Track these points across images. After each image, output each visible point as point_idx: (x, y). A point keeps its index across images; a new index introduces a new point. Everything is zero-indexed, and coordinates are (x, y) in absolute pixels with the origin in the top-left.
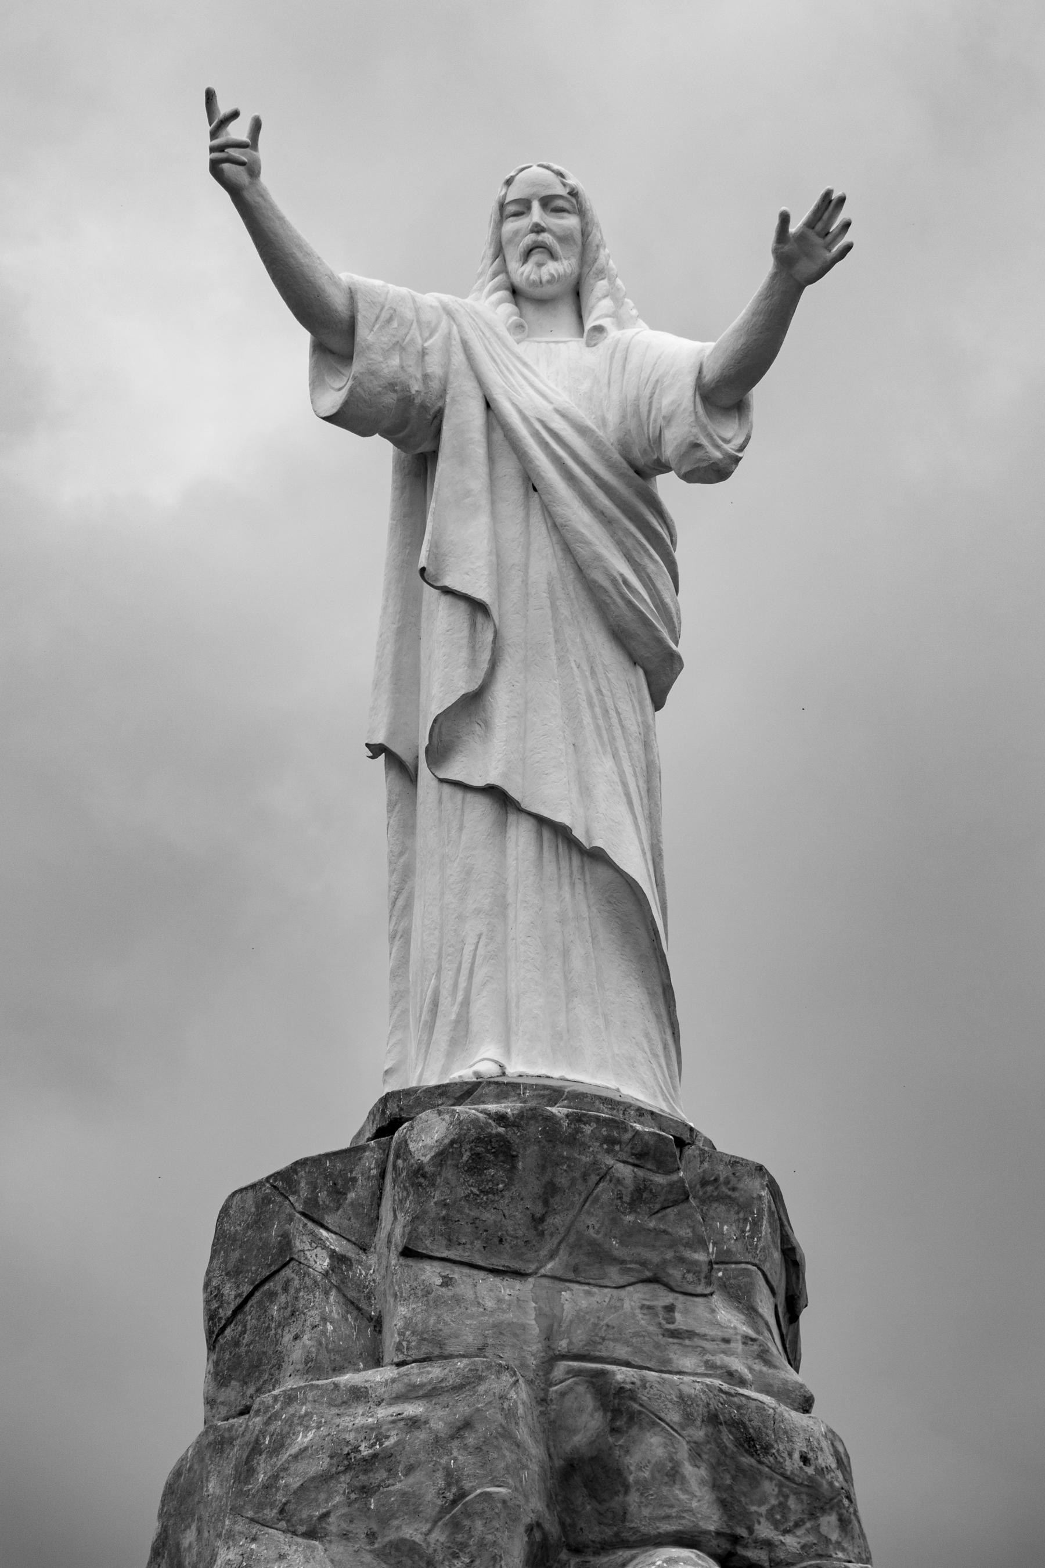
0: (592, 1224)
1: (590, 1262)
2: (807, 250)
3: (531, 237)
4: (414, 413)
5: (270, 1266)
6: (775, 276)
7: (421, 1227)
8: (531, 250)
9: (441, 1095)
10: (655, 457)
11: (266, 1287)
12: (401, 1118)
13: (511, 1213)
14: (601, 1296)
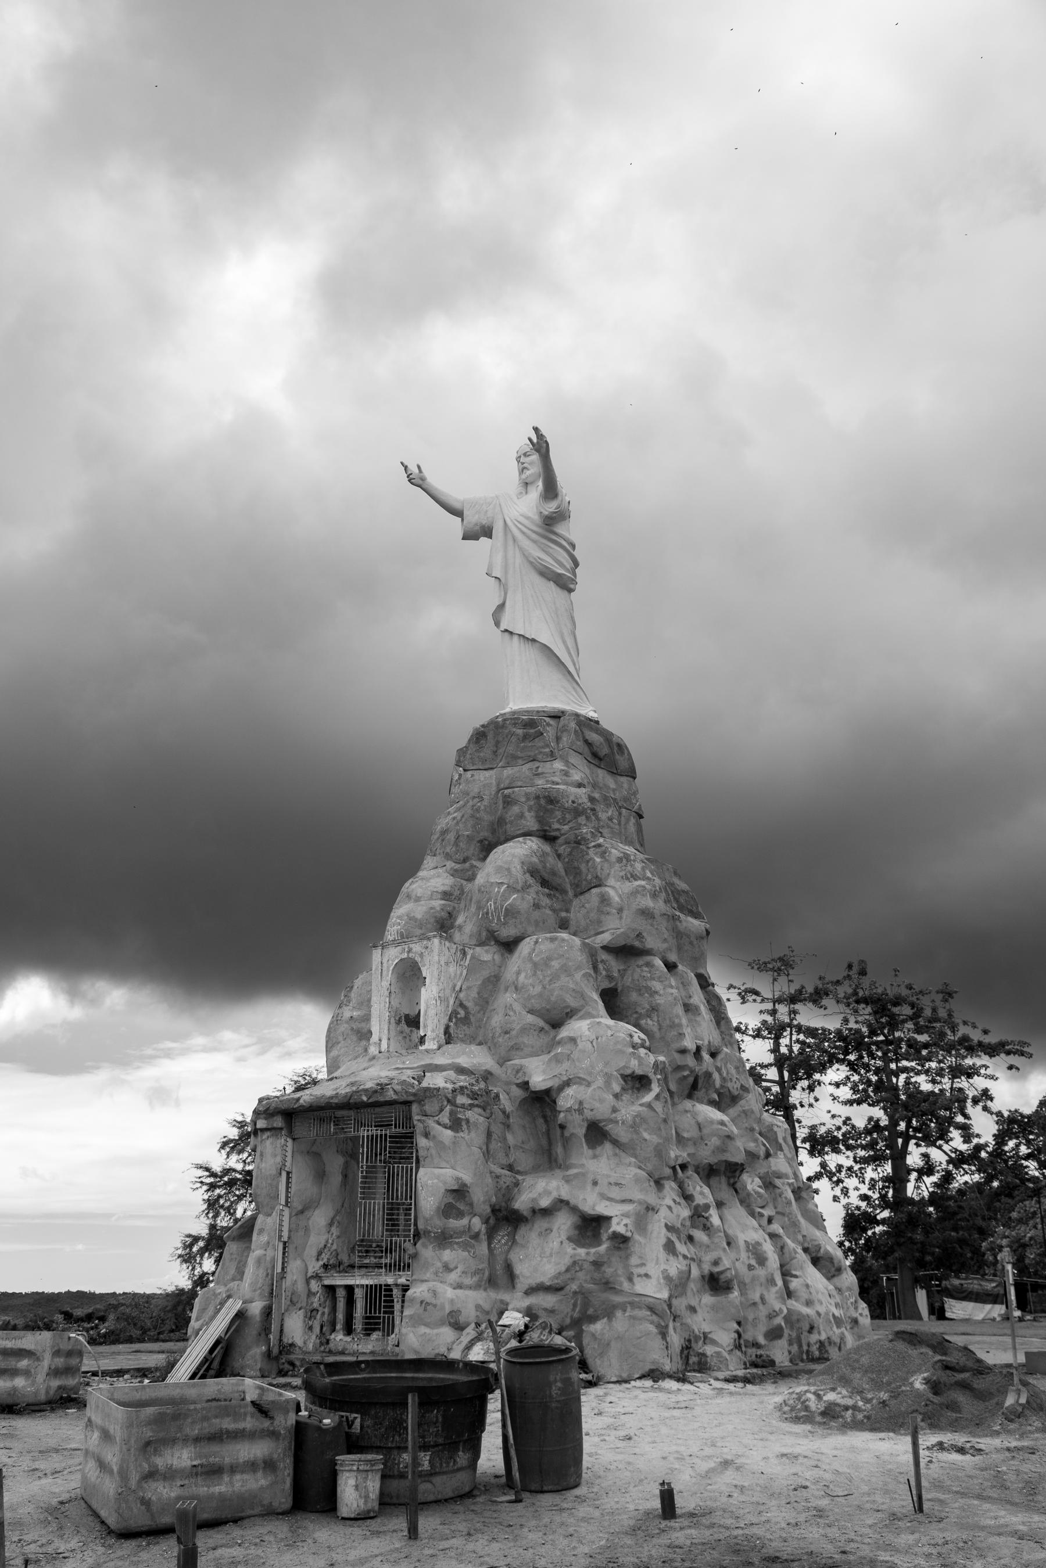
0: (511, 749)
1: (512, 760)
13: (486, 752)
14: (516, 769)
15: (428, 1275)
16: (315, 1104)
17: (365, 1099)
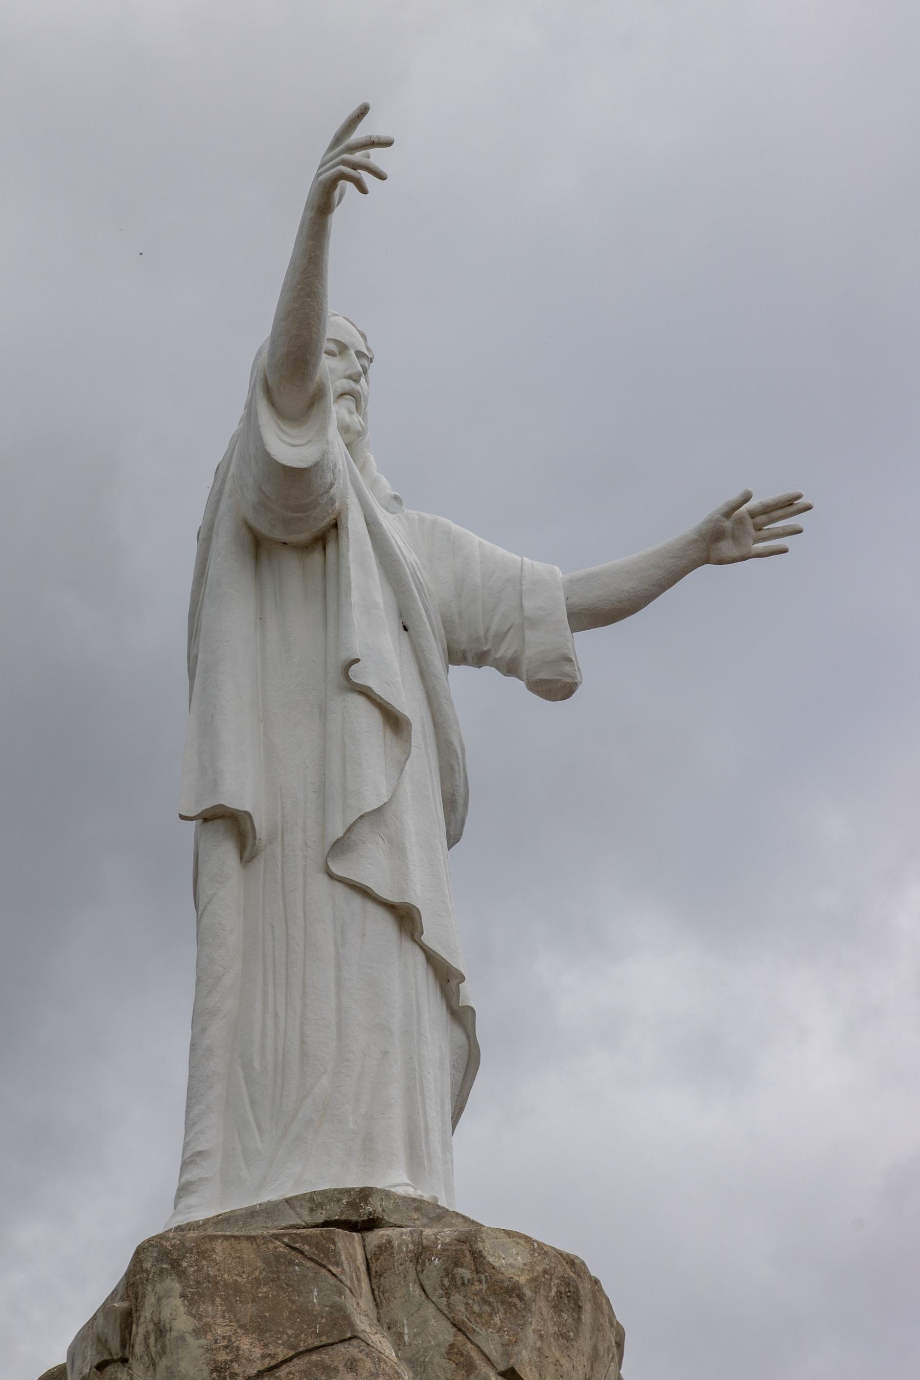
2: (738, 533)
3: (348, 384)
4: (325, 499)
5: (319, 1335)
6: (696, 541)
7: (525, 1353)
8: (342, 395)
9: (417, 1209)
10: (485, 649)
11: (315, 1357)
12: (382, 1219)
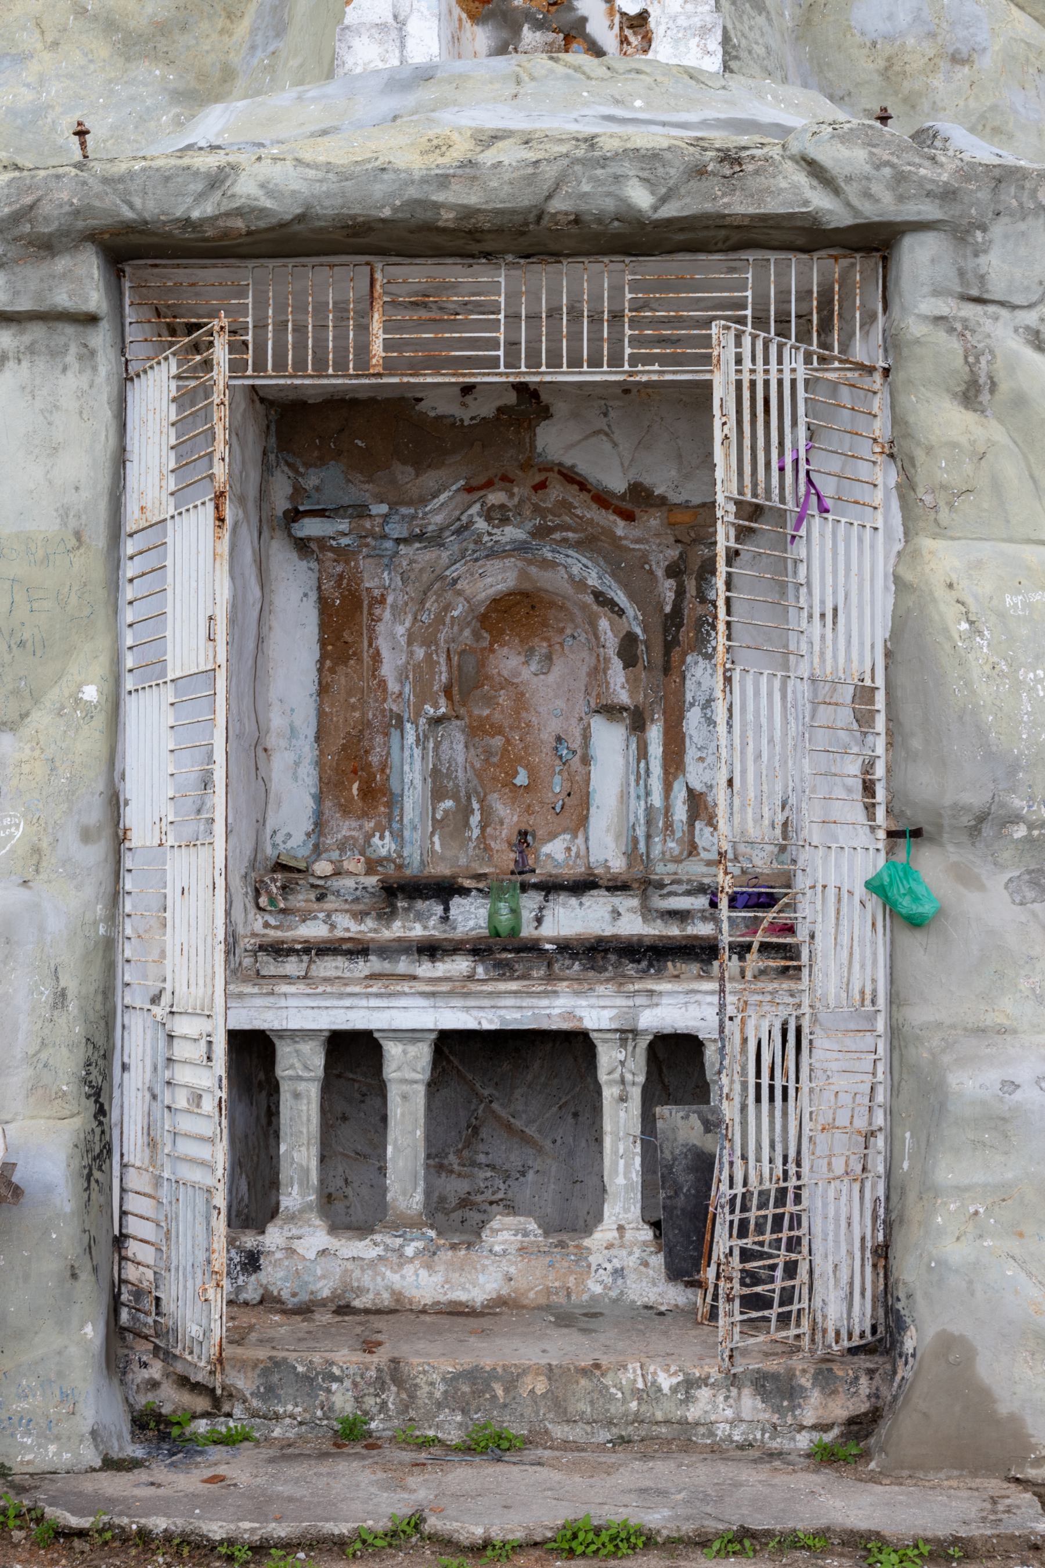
15: (1009, 1008)
16: (328, 209)
17: (641, 198)
